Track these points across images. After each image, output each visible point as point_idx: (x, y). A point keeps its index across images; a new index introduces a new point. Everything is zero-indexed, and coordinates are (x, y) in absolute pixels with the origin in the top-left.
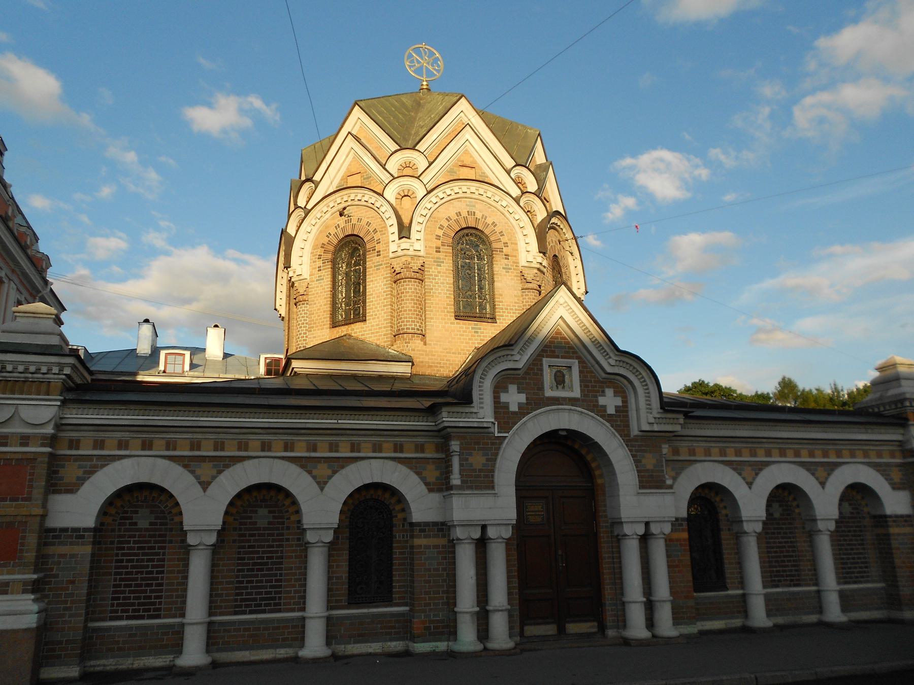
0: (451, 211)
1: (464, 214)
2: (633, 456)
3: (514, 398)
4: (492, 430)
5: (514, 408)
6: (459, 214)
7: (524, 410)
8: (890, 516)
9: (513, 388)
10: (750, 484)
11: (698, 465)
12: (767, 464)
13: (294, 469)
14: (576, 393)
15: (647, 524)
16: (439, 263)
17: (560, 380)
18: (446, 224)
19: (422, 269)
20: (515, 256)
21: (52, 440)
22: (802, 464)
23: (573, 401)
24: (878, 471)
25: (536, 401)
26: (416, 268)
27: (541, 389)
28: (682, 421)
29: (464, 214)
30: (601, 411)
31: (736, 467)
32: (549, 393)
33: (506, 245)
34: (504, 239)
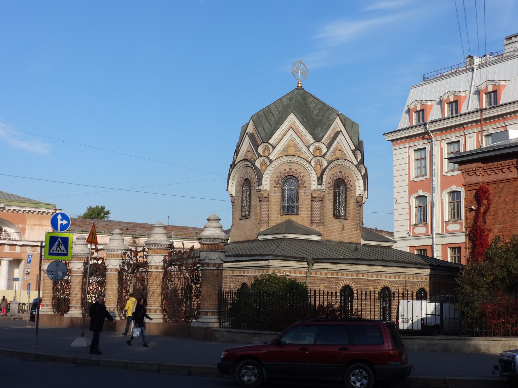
1: (288, 170)
6: (285, 170)
19: (268, 196)
20: (309, 186)
26: (265, 196)
29: (288, 170)
33: (305, 181)
34: (304, 179)
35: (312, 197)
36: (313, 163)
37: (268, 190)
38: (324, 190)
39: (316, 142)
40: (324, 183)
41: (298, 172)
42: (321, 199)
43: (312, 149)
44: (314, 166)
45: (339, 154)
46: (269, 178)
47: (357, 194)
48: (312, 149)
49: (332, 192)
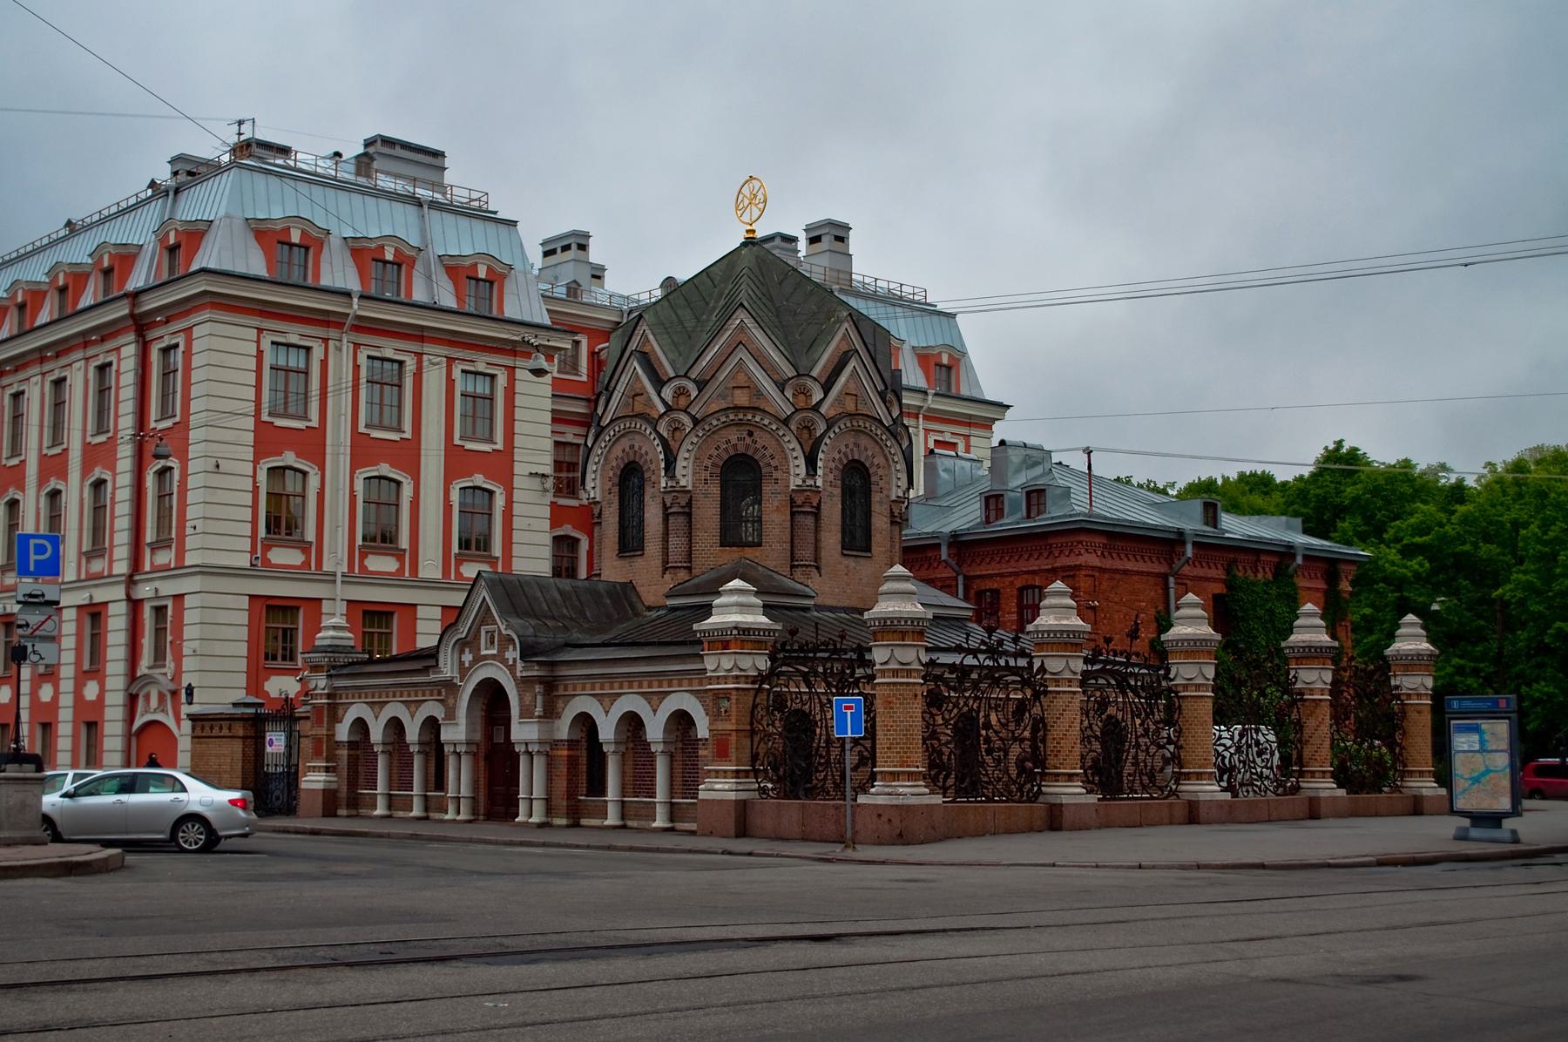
0: (617, 451)
1: (627, 449)
2: (520, 695)
3: (468, 657)
4: (455, 681)
5: (467, 665)
7: (473, 663)
8: (701, 740)
9: (467, 650)
10: (607, 712)
11: (577, 698)
12: (620, 695)
13: (402, 707)
14: (495, 652)
15: (526, 744)
16: (610, 504)
17: (492, 643)
18: (614, 464)
21: (329, 696)
22: (642, 694)
23: (493, 657)
24: (698, 698)
25: (478, 659)
27: (479, 650)
28: (536, 668)
30: (504, 661)
31: (599, 697)
32: (484, 652)
35: (665, 508)
36: (663, 429)
37: (598, 499)
38: (690, 488)
39: (677, 377)
40: (679, 472)
41: (643, 452)
42: (687, 510)
43: (668, 393)
44: (665, 435)
45: (742, 398)
46: (599, 472)
47: (792, 487)
48: (668, 393)
49: (715, 490)
